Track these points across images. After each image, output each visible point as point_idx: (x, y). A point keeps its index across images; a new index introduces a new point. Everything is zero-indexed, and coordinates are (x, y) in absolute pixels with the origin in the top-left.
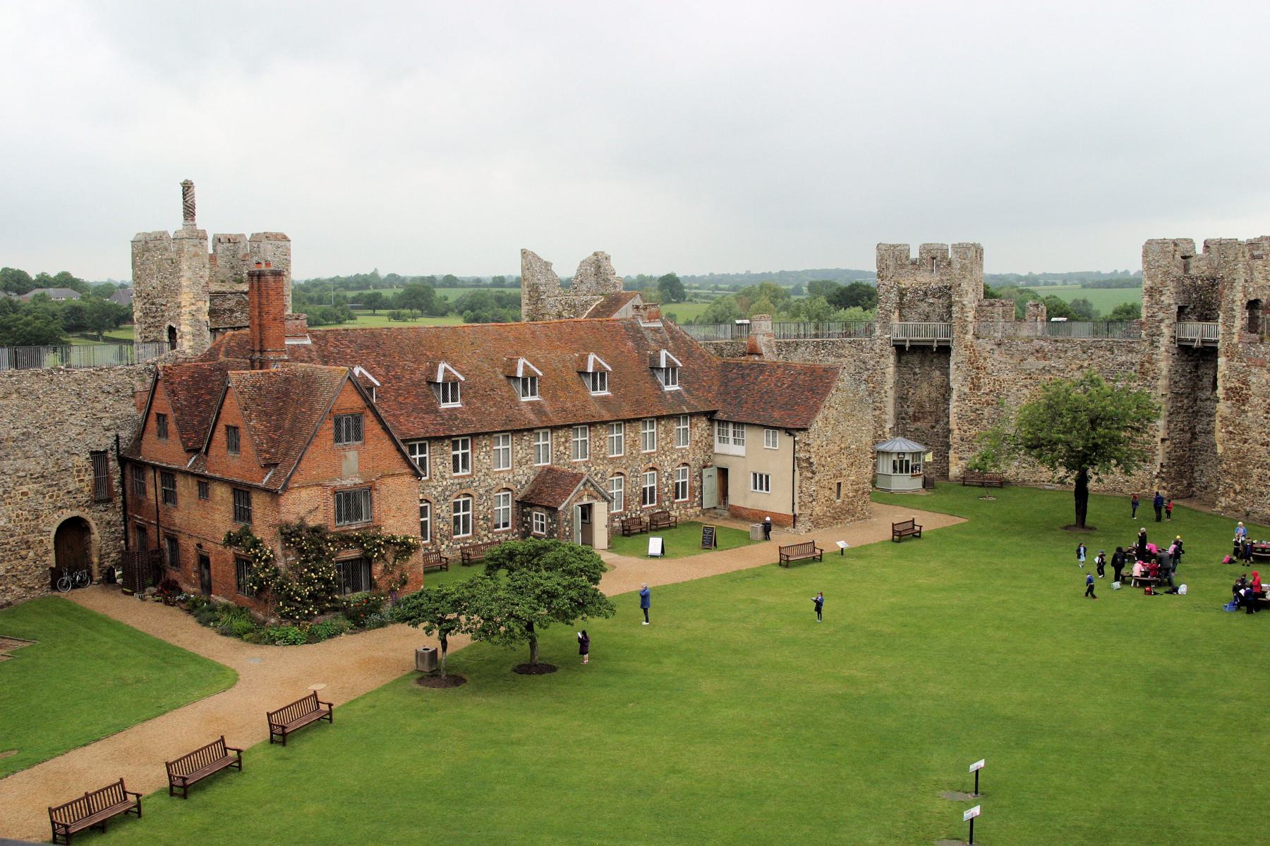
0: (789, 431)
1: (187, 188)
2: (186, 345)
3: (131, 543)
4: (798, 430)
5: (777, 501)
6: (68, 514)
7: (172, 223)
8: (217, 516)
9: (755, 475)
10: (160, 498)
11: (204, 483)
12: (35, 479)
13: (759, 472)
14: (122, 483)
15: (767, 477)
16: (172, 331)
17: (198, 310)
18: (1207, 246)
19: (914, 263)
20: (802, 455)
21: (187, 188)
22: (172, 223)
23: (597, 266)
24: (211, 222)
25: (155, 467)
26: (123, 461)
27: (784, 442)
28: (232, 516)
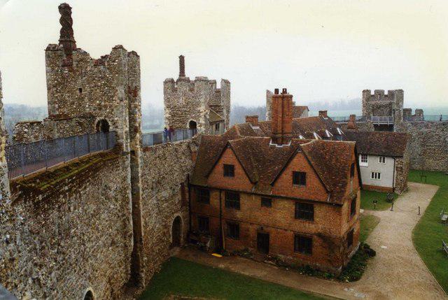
0: (394, 157)
1: (182, 59)
2: (201, 129)
3: (192, 224)
4: (396, 157)
5: (386, 181)
6: (176, 215)
7: (176, 77)
8: (278, 215)
9: (373, 173)
10: (223, 205)
11: (267, 201)
12: (166, 201)
13: (375, 172)
14: (190, 198)
15: (379, 174)
16: (193, 125)
17: (207, 113)
18: (389, 91)
19: (372, 96)
20: (399, 166)
21: (182, 59)
22: (176, 77)
23: (291, 97)
24: (191, 74)
25: (221, 190)
26: (190, 186)
27: (390, 162)
28: (293, 216)
